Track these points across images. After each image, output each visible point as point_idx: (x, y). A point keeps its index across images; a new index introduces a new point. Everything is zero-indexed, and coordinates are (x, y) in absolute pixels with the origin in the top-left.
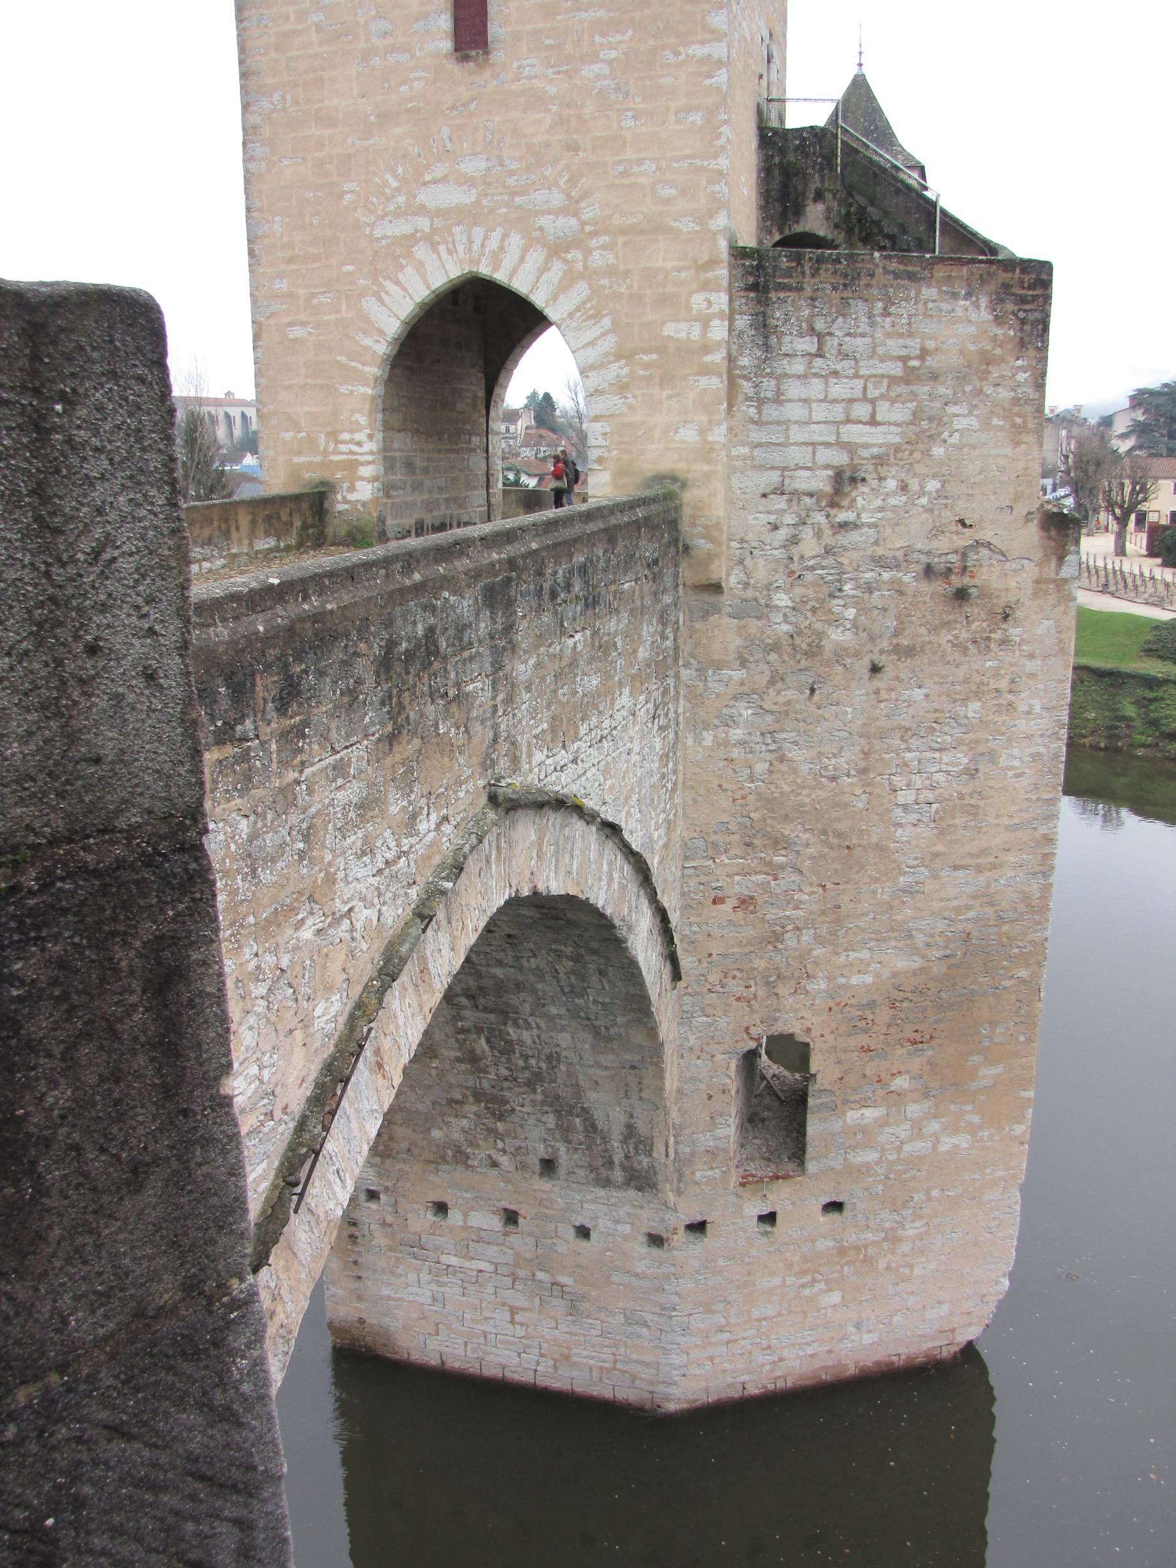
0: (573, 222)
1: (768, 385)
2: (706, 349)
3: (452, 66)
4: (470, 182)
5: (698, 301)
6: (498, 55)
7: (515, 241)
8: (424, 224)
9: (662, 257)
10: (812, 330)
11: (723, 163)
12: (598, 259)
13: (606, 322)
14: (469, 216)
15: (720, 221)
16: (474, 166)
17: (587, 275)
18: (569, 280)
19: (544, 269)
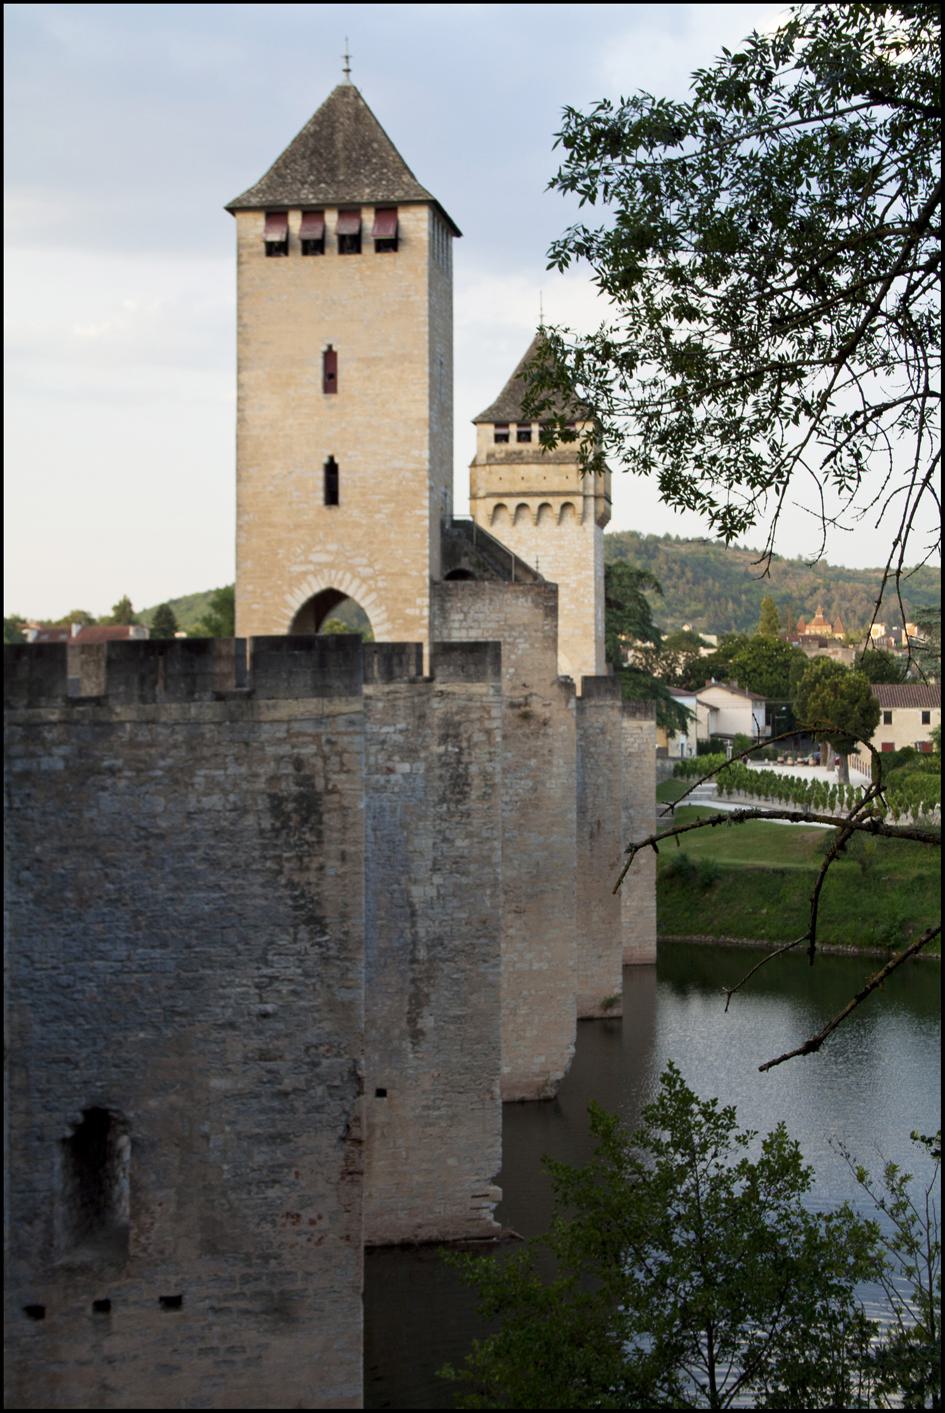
0: (371, 570)
2: (422, 618)
3: (325, 509)
4: (328, 552)
5: (419, 601)
7: (348, 576)
8: (311, 567)
9: (405, 584)
10: (462, 612)
12: (381, 584)
13: (383, 608)
14: (331, 566)
16: (333, 547)
17: (377, 590)
18: (370, 591)
19: (359, 587)
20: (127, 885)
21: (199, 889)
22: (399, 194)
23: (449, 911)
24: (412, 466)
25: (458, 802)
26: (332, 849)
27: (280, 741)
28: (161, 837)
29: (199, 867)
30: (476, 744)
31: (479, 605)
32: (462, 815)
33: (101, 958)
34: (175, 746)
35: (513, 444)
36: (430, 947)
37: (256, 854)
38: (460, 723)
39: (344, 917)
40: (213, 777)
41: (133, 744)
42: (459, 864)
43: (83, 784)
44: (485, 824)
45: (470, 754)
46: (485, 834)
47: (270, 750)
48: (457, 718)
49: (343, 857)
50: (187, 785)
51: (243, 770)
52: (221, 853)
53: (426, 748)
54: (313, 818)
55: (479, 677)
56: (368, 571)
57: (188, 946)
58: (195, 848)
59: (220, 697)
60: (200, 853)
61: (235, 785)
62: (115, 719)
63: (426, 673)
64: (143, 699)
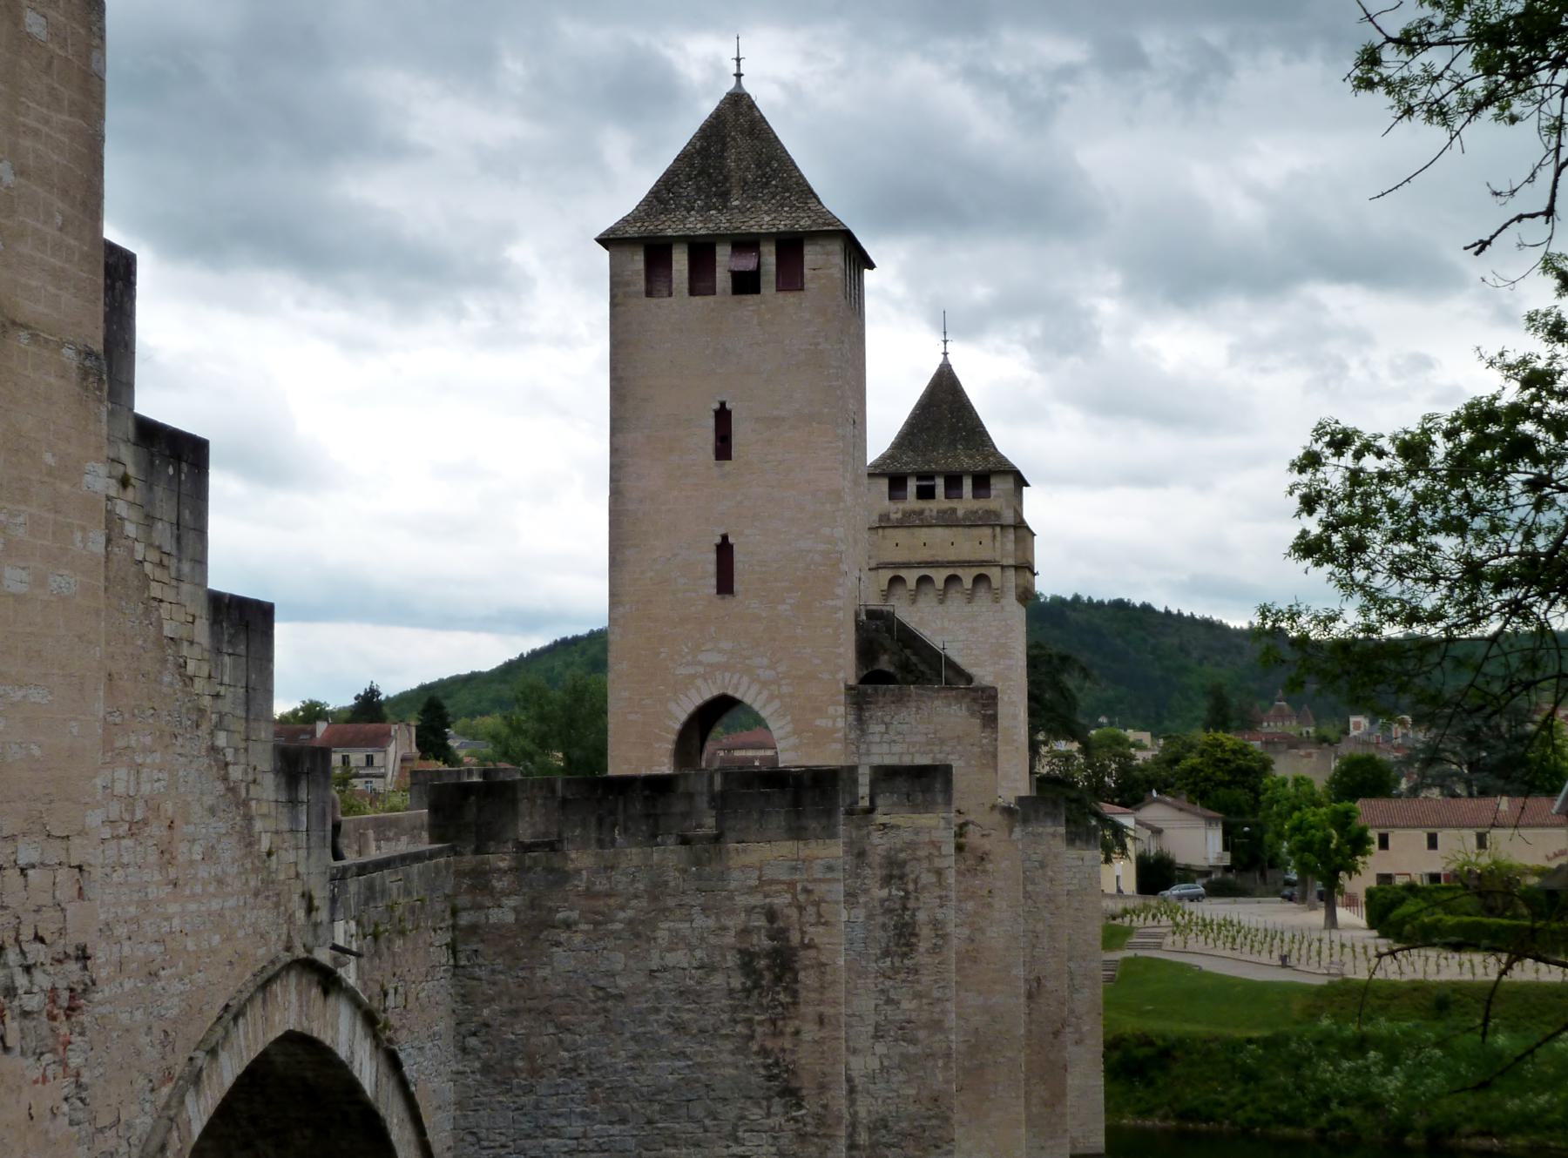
1: (863, 747)
3: (717, 600)
5: (831, 710)
6: (739, 597)
7: (745, 679)
8: (701, 670)
10: (883, 722)
11: (842, 650)
12: (785, 689)
15: (841, 675)
16: (726, 645)
18: (771, 698)
20: (583, 1053)
21: (663, 1057)
22: (805, 223)
23: (894, 1087)
24: (821, 547)
25: (905, 955)
26: (808, 1011)
27: (752, 890)
28: (621, 997)
29: (662, 1033)
30: (924, 887)
31: (904, 714)
32: (909, 971)
33: (554, 1136)
34: (636, 897)
35: (911, 502)
36: (872, 1130)
37: (725, 1017)
38: (905, 862)
39: (823, 1088)
40: (677, 931)
41: (589, 894)
42: (905, 1030)
43: (535, 938)
44: (936, 981)
45: (917, 899)
46: (936, 994)
47: (741, 900)
48: (902, 855)
49: (821, 1020)
50: (649, 940)
51: (711, 922)
52: (686, 1016)
53: (866, 891)
54: (788, 977)
55: (927, 807)
56: (769, 674)
57: (650, 1122)
58: (657, 1011)
59: (685, 841)
60: (663, 1016)
61: (702, 939)
62: (570, 866)
63: (865, 803)
64: (601, 844)
